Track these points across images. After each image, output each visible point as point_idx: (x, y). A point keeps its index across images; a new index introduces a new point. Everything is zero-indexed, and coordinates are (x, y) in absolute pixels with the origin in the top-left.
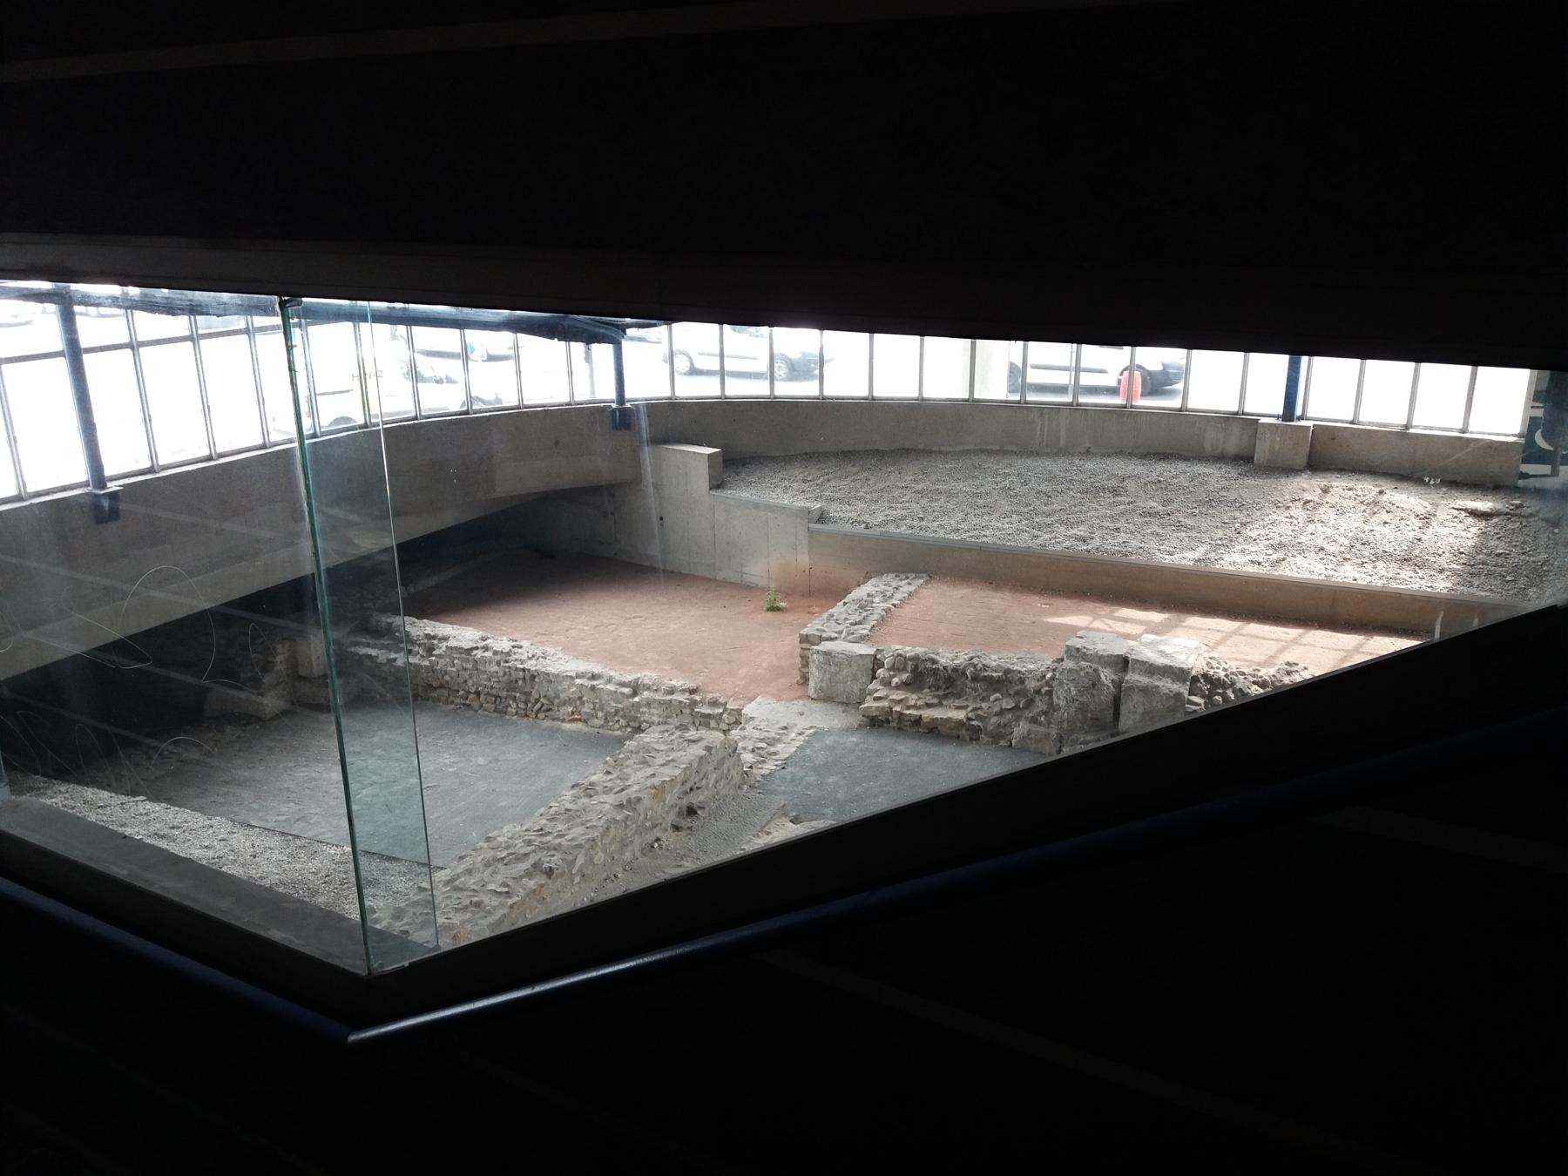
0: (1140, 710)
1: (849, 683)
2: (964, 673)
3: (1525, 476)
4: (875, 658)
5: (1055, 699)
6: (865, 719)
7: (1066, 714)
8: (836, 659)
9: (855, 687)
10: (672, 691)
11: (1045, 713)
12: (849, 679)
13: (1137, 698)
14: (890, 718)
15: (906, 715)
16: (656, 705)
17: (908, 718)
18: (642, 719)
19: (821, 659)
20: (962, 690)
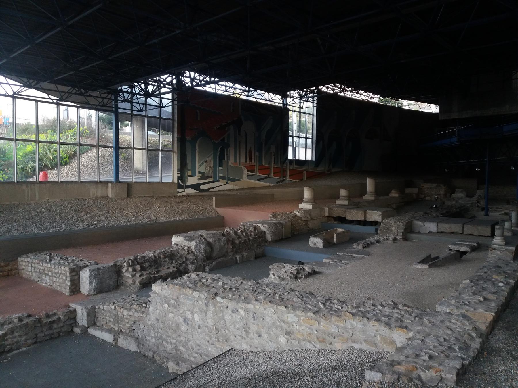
0: (218, 248)
1: (108, 281)
2: (159, 257)
3: (179, 192)
4: (116, 265)
5: (195, 253)
6: (141, 285)
7: (202, 256)
8: (104, 270)
9: (111, 282)
10: (20, 319)
11: (195, 259)
12: (108, 279)
13: (217, 243)
14: (151, 281)
15: (157, 276)
16: (18, 330)
17: (158, 278)
18: (6, 344)
19: (96, 273)
20: (160, 264)
